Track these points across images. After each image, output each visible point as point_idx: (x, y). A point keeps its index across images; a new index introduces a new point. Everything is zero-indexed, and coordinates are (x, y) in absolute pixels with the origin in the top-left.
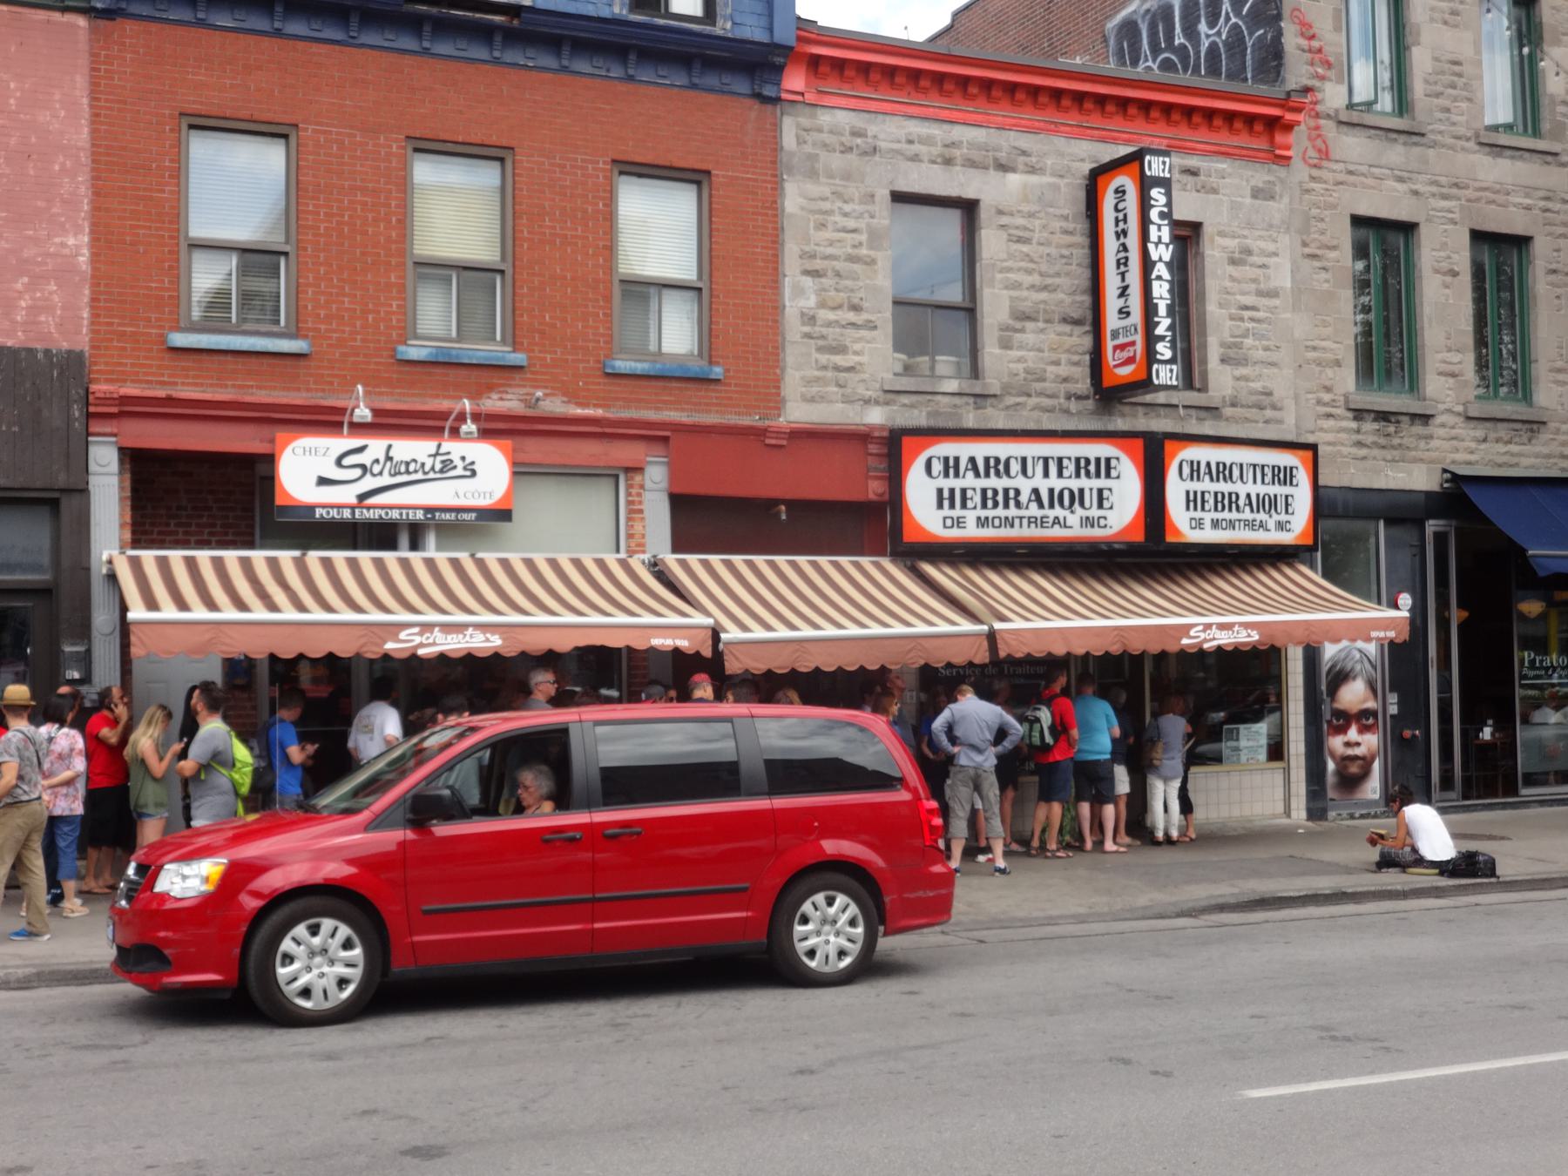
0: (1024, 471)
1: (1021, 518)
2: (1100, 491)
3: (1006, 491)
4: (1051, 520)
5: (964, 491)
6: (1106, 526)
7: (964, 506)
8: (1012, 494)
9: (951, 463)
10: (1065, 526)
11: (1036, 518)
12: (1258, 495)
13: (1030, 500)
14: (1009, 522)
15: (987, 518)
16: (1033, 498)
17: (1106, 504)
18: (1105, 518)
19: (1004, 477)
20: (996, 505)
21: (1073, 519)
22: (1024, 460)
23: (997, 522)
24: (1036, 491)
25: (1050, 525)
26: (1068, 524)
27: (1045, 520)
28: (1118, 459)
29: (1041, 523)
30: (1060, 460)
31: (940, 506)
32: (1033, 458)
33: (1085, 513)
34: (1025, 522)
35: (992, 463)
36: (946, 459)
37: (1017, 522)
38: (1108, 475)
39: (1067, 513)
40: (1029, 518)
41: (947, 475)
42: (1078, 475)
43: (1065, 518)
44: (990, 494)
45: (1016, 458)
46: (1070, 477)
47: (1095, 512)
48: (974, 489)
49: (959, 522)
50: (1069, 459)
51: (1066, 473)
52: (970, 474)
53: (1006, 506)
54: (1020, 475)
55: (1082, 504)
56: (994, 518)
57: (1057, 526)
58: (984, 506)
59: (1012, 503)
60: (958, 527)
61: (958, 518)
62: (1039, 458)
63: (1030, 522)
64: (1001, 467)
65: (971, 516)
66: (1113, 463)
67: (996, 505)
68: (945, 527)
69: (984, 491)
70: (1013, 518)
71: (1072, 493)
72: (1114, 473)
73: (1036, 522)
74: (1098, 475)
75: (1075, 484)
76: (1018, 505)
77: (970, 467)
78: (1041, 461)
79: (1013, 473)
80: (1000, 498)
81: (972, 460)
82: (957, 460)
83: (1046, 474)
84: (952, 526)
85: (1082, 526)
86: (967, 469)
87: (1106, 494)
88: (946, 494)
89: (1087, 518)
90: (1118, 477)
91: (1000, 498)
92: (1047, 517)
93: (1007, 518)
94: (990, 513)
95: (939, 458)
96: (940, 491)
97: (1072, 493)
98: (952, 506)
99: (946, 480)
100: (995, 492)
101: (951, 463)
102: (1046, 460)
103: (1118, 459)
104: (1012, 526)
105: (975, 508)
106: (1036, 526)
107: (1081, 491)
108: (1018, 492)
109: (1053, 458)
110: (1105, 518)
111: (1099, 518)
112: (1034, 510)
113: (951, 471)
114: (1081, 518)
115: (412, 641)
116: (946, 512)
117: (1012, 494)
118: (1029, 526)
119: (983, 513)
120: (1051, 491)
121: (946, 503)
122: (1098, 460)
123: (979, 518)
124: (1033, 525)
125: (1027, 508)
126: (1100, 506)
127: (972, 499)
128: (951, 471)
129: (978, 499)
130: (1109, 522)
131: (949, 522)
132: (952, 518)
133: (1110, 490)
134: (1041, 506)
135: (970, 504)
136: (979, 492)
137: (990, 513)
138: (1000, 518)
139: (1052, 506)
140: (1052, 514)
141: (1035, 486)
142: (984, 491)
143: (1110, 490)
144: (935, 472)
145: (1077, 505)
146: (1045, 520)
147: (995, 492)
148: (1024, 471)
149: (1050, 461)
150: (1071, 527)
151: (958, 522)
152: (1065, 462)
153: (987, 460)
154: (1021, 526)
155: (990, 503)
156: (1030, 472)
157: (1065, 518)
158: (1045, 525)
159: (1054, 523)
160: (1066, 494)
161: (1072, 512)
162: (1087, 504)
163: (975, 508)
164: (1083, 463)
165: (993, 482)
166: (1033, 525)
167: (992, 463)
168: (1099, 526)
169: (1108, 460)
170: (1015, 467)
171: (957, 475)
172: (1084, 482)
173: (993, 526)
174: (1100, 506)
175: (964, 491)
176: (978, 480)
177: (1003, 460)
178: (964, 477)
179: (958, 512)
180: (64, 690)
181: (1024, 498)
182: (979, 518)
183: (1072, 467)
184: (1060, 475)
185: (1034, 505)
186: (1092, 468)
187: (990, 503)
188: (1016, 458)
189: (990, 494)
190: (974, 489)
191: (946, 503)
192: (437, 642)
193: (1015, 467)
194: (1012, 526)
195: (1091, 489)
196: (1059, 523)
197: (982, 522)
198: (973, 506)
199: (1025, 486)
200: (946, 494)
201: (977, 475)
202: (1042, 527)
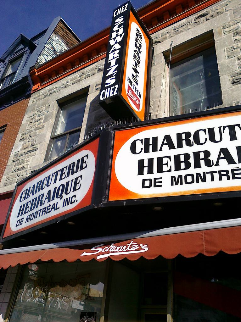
0: (212, 138)
1: (212, 173)
3: (196, 154)
5: (160, 160)
7: (160, 170)
8: (202, 155)
11: (227, 171)
13: (219, 158)
15: (180, 177)
22: (211, 131)
23: (189, 179)
31: (141, 172)
32: (220, 128)
34: (216, 176)
35: (184, 137)
36: (147, 140)
37: (208, 176)
40: (220, 172)
44: (182, 158)
45: (205, 131)
48: (169, 157)
49: (156, 183)
52: (166, 147)
53: (197, 165)
58: (178, 168)
59: (202, 162)
60: (155, 186)
61: (155, 179)
62: (225, 127)
64: (192, 139)
65: (166, 177)
67: (188, 166)
68: (144, 187)
69: (177, 157)
70: (204, 174)
73: (227, 175)
77: (165, 142)
78: (227, 129)
79: (202, 141)
80: (192, 160)
81: (168, 138)
82: (155, 139)
84: (150, 186)
86: (163, 144)
88: (146, 163)
91: (192, 160)
93: (198, 175)
94: (183, 173)
96: (141, 162)
98: (150, 171)
104: (204, 180)
105: (170, 170)
106: (228, 178)
108: (207, 154)
112: (224, 165)
116: (146, 176)
117: (202, 155)
118: (221, 179)
119: (177, 174)
121: (146, 170)
123: (173, 178)
124: (224, 178)
125: (217, 164)
127: (167, 164)
129: (172, 163)
131: (147, 183)
135: (165, 168)
136: (173, 158)
137: (183, 173)
142: (177, 157)
144: (138, 150)
147: (187, 156)
151: (155, 182)
153: (179, 136)
154: (213, 179)
155: (183, 165)
156: (217, 138)
163: (170, 170)
165: (186, 149)
166: (224, 178)
167: (184, 137)
170: (203, 137)
171: (155, 150)
173: (186, 182)
175: (160, 160)
178: (161, 150)
179: (155, 175)
181: (213, 158)
182: (173, 178)
187: (183, 165)
188: (205, 131)
189: (182, 158)
191: (146, 170)
194: (204, 180)
197: (175, 181)
198: (168, 169)
199: (214, 149)
200: (146, 163)
201: (171, 147)
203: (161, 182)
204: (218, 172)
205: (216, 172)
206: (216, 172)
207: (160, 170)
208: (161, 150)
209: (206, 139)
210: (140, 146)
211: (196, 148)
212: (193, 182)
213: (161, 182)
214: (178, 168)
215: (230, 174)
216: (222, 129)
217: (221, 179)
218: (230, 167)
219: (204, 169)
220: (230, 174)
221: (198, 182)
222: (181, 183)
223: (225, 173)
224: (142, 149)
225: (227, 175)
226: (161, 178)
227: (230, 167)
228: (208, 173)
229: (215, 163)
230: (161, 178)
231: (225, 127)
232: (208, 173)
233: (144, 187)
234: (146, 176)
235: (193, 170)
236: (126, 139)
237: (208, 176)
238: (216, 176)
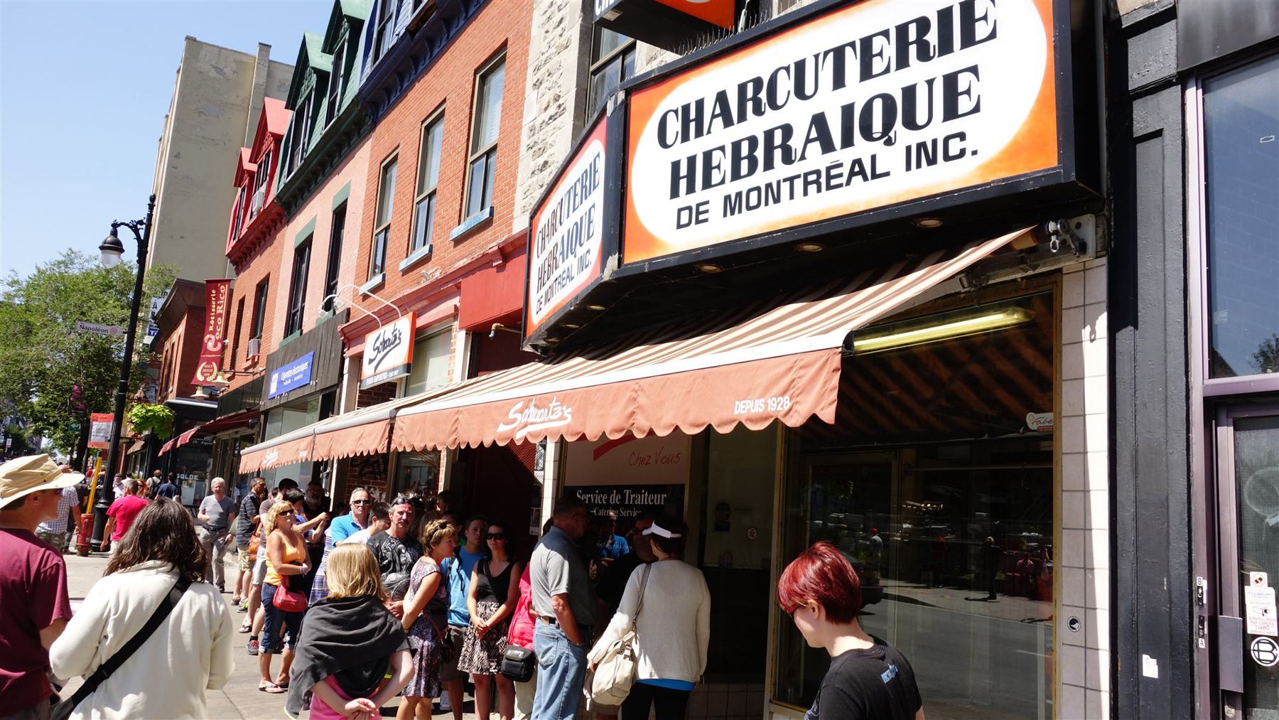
1: (791, 180)
4: (845, 170)
6: (962, 153)
7: (707, 184)
10: (875, 176)
13: (808, 141)
14: (772, 194)
17: (964, 104)
18: (962, 136)
21: (890, 158)
23: (753, 201)
24: (819, 121)
25: (843, 180)
29: (825, 180)
31: (675, 193)
32: (817, 57)
33: (913, 138)
34: (799, 184)
37: (785, 187)
39: (878, 147)
40: (806, 175)
43: (873, 158)
47: (939, 129)
49: (698, 215)
53: (769, 165)
57: (857, 180)
62: (826, 53)
63: (806, 184)
64: (763, 95)
65: (715, 197)
67: (752, 169)
68: (679, 226)
73: (817, 182)
75: (893, 84)
83: (839, 82)
85: (908, 168)
86: (714, 116)
87: (964, 81)
91: (760, 153)
92: (840, 165)
94: (743, 185)
96: (676, 166)
98: (691, 189)
100: (753, 141)
105: (723, 182)
106: (819, 190)
107: (909, 93)
110: (962, 136)
112: (816, 159)
114: (908, 149)
118: (806, 193)
120: (848, 111)
124: (812, 188)
125: (803, 158)
126: (951, 112)
130: (969, 145)
131: (685, 216)
133: (974, 70)
134: (827, 147)
135: (716, 177)
139: (848, 141)
140: (845, 157)
143: (974, 70)
148: (800, 92)
150: (887, 174)
157: (873, 158)
158: (833, 182)
159: (852, 174)
160: (878, 106)
161: (889, 142)
162: (921, 118)
166: (812, 188)
168: (947, 158)
170: (785, 84)
174: (951, 112)
178: (709, 132)
180: (643, 491)
186: (932, 37)
193: (785, 84)
195: (930, 83)
196: (862, 172)
197: (732, 205)
199: (798, 115)
201: (728, 122)
205: (798, 176)
206: (798, 176)
208: (709, 132)
209: (789, 92)
211: (772, 119)
215: (823, 180)
217: (806, 193)
219: (781, 171)
220: (823, 180)
222: (740, 211)
223: (812, 178)
226: (707, 203)
228: (785, 180)
230: (707, 203)
231: (826, 53)
232: (785, 180)
234: (685, 200)
235: (761, 178)
237: (785, 187)
238: (799, 184)
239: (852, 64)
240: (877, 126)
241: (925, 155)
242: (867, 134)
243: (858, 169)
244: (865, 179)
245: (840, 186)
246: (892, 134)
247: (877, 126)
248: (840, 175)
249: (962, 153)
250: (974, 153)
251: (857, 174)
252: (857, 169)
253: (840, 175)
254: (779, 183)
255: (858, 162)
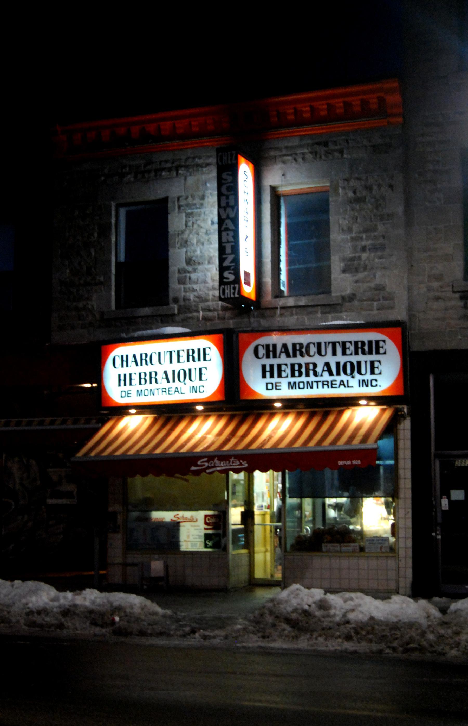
1: (317, 382)
2: (372, 363)
4: (338, 383)
5: (279, 366)
6: (376, 386)
7: (280, 376)
8: (311, 367)
9: (271, 349)
10: (348, 387)
11: (328, 382)
12: (174, 371)
13: (323, 370)
14: (310, 385)
15: (295, 383)
16: (326, 369)
17: (376, 371)
18: (376, 380)
19: (306, 356)
20: (300, 374)
21: (354, 382)
22: (319, 345)
23: (301, 385)
24: (327, 365)
25: (337, 386)
26: (350, 385)
27: (334, 383)
28: (384, 341)
29: (332, 385)
30: (344, 344)
31: (264, 376)
32: (325, 343)
33: (361, 378)
34: (320, 384)
36: (268, 346)
37: (315, 384)
38: (378, 353)
39: (349, 378)
40: (323, 382)
41: (268, 357)
42: (357, 353)
43: (348, 381)
44: (296, 367)
46: (351, 354)
47: (368, 377)
48: (286, 365)
49: (276, 387)
50: (350, 342)
51: (348, 352)
52: (283, 355)
53: (308, 375)
54: (317, 355)
55: (360, 372)
56: (299, 383)
57: (342, 387)
58: (293, 375)
59: (311, 373)
60: (276, 389)
61: (276, 383)
62: (329, 343)
63: (323, 385)
64: (304, 350)
65: (284, 383)
66: (381, 344)
67: (300, 374)
68: (267, 389)
69: (293, 366)
71: (352, 364)
72: (382, 351)
73: (328, 385)
74: (370, 353)
75: (354, 359)
76: (315, 374)
77: (283, 350)
78: (331, 345)
79: (312, 353)
80: (303, 370)
82: (275, 346)
83: (334, 354)
84: (272, 389)
85: (359, 386)
87: (376, 364)
88: (268, 368)
89: (364, 381)
90: (385, 353)
91: (303, 370)
92: (336, 381)
93: (308, 383)
95: (263, 346)
96: (264, 367)
97: (352, 364)
99: (268, 360)
101: (271, 349)
102: (334, 344)
103: (384, 341)
104: (312, 387)
106: (328, 387)
107: (359, 363)
108: (315, 365)
109: (339, 342)
110: (376, 380)
111: (372, 380)
112: (326, 377)
113: (271, 354)
114: (359, 381)
115: (204, 465)
116: (268, 379)
117: (311, 367)
118: (323, 387)
119: (292, 380)
120: (338, 364)
121: (268, 374)
122: (370, 342)
124: (326, 387)
125: (322, 375)
126: (372, 373)
128: (271, 354)
129: (289, 371)
130: (378, 383)
132: (272, 384)
133: (379, 362)
134: (331, 374)
135: (283, 374)
137: (297, 380)
138: (304, 382)
140: (338, 379)
141: (327, 361)
142: (293, 366)
143: (379, 362)
144: (260, 355)
145: (356, 373)
146: (334, 383)
147: (300, 366)
148: (319, 353)
149: (337, 344)
151: (276, 386)
152: (348, 345)
153: (294, 345)
154: (318, 387)
155: (297, 373)
156: (323, 353)
157: (348, 381)
158: (334, 386)
159: (340, 385)
161: (353, 377)
162: (363, 371)
163: (287, 377)
164: (360, 345)
165: (299, 360)
166: (326, 387)
168: (372, 386)
169: (377, 342)
170: (313, 349)
171: (275, 356)
172: (361, 358)
173: (299, 388)
174: (372, 373)
175: (279, 366)
176: (289, 359)
177: (305, 345)
178: (279, 357)
181: (319, 370)
182: (289, 383)
183: (352, 348)
184: (344, 353)
185: (326, 374)
186: (366, 348)
187: (297, 373)
188: (314, 344)
189: (296, 367)
190: (286, 365)
191: (268, 374)
192: (216, 465)
193: (313, 349)
194: (312, 387)
195: (366, 362)
196: (344, 385)
200: (268, 368)
201: (288, 356)
202: (332, 387)
203: (280, 386)
204: (322, 382)
205: (320, 381)
206: (320, 381)
207: (280, 376)
209: (315, 352)
210: (262, 352)
211: (307, 359)
212: (304, 388)
213: (280, 386)
214: (293, 375)
215: (330, 384)
216: (327, 344)
217: (323, 387)
218: (330, 379)
220: (330, 384)
221: (307, 388)
222: (296, 388)
224: (264, 354)
225: (328, 385)
227: (330, 379)
228: (315, 382)
229: (320, 374)
232: (315, 382)
233: (267, 389)
236: (250, 343)
237: (315, 384)
238: (320, 384)
239: (339, 350)
240: (349, 371)
241: (365, 383)
242: (345, 373)
243: (342, 383)
244: (345, 387)
245: (336, 387)
246: (354, 375)
247: (349, 371)
248: (336, 384)
249: (376, 386)
250: (380, 386)
251: (342, 385)
252: (342, 383)
253: (336, 384)
254: (312, 382)
255: (342, 381)
